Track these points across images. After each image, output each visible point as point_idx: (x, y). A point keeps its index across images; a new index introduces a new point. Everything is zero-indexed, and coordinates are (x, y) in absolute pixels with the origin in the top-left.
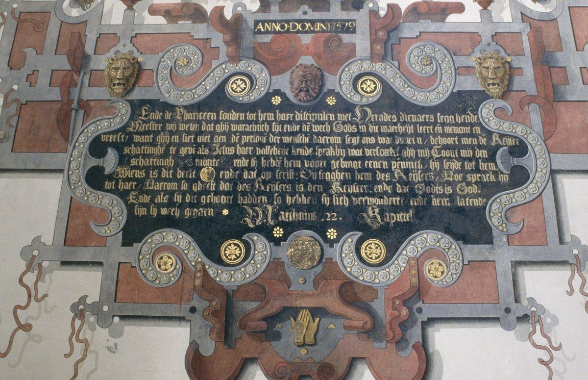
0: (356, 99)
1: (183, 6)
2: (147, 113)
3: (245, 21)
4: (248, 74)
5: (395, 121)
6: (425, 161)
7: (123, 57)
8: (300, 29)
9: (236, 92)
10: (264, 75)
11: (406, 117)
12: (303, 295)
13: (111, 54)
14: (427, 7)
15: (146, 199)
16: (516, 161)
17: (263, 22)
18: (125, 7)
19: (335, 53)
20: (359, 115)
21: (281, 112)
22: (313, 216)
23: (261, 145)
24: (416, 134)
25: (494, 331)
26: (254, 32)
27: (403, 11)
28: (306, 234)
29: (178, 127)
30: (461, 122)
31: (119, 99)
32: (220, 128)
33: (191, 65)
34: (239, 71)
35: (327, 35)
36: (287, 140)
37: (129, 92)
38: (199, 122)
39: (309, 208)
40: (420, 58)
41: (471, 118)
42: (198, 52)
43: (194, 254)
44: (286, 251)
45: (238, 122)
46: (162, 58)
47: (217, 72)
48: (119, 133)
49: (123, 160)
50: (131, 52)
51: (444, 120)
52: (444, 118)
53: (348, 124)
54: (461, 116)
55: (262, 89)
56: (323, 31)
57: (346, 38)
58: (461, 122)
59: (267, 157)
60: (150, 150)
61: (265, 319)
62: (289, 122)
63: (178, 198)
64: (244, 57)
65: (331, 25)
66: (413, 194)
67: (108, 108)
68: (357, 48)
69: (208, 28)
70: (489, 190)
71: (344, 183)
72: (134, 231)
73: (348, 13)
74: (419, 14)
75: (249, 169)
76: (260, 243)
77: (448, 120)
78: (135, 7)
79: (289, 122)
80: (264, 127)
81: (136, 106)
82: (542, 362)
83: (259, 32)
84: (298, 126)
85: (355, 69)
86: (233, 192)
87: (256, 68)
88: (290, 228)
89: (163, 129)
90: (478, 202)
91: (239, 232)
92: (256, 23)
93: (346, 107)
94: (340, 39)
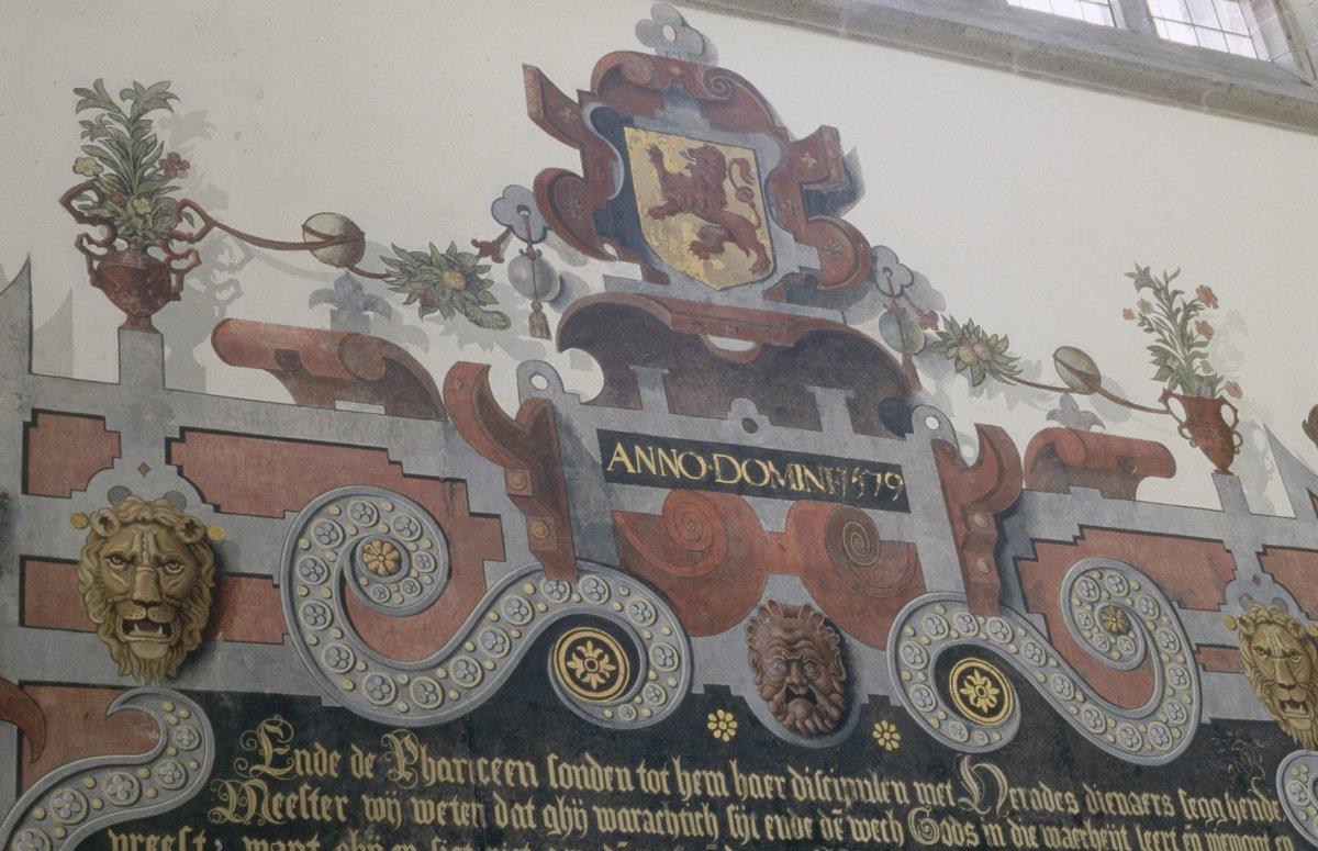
0: (952, 733)
1: (343, 342)
2: (281, 751)
3: (569, 430)
4: (614, 625)
5: (1076, 811)
7: (147, 515)
8: (748, 479)
9: (587, 687)
10: (666, 631)
11: (1101, 800)
13: (95, 497)
14: (1081, 449)
17: (630, 440)
18: (121, 317)
20: (973, 786)
21: (746, 769)
26: (606, 473)
27: (1022, 455)
29: (408, 811)
30: (1242, 819)
31: (155, 687)
33: (414, 573)
34: (580, 609)
35: (829, 508)
37: (194, 659)
38: (481, 794)
40: (1098, 607)
42: (429, 525)
45: (615, 799)
46: (301, 535)
48: (181, 827)
50: (175, 501)
51: (1198, 812)
52: (1197, 807)
53: (951, 818)
54: (1237, 800)
55: (672, 682)
56: (816, 495)
57: (886, 523)
58: (1242, 819)
62: (776, 806)
64: (588, 560)
65: (834, 474)
67: (116, 721)
68: (923, 561)
69: (446, 438)
73: (873, 442)
74: (1064, 466)
77: (1210, 816)
78: (157, 319)
79: (776, 806)
80: (702, 821)
81: (235, 719)
83: (620, 476)
84: (808, 821)
87: (633, 604)
89: (355, 814)
92: (608, 440)
93: (936, 762)
94: (871, 529)
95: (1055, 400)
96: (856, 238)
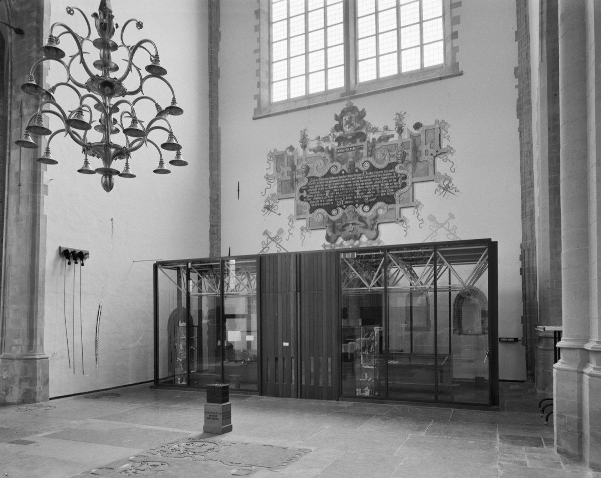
0: (363, 169)
6: (380, 184)
12: (350, 221)
15: (314, 202)
16: (403, 181)
19: (358, 156)
22: (352, 202)
23: (340, 185)
24: (378, 177)
25: (394, 224)
28: (351, 206)
32: (330, 182)
36: (346, 183)
39: (351, 200)
41: (393, 170)
43: (326, 214)
44: (346, 211)
45: (334, 180)
47: (328, 166)
49: (308, 193)
50: (306, 164)
57: (361, 151)
59: (341, 188)
60: (314, 190)
61: (342, 227)
63: (321, 201)
66: (376, 193)
70: (396, 190)
71: (360, 192)
72: (312, 210)
75: (337, 192)
76: (340, 209)
81: (309, 178)
82: (405, 231)
85: (363, 160)
86: (334, 198)
87: (338, 164)
88: (347, 205)
90: (393, 193)
91: (335, 207)
92: (337, 150)
93: (360, 172)
95: (382, 133)
96: (364, 121)
